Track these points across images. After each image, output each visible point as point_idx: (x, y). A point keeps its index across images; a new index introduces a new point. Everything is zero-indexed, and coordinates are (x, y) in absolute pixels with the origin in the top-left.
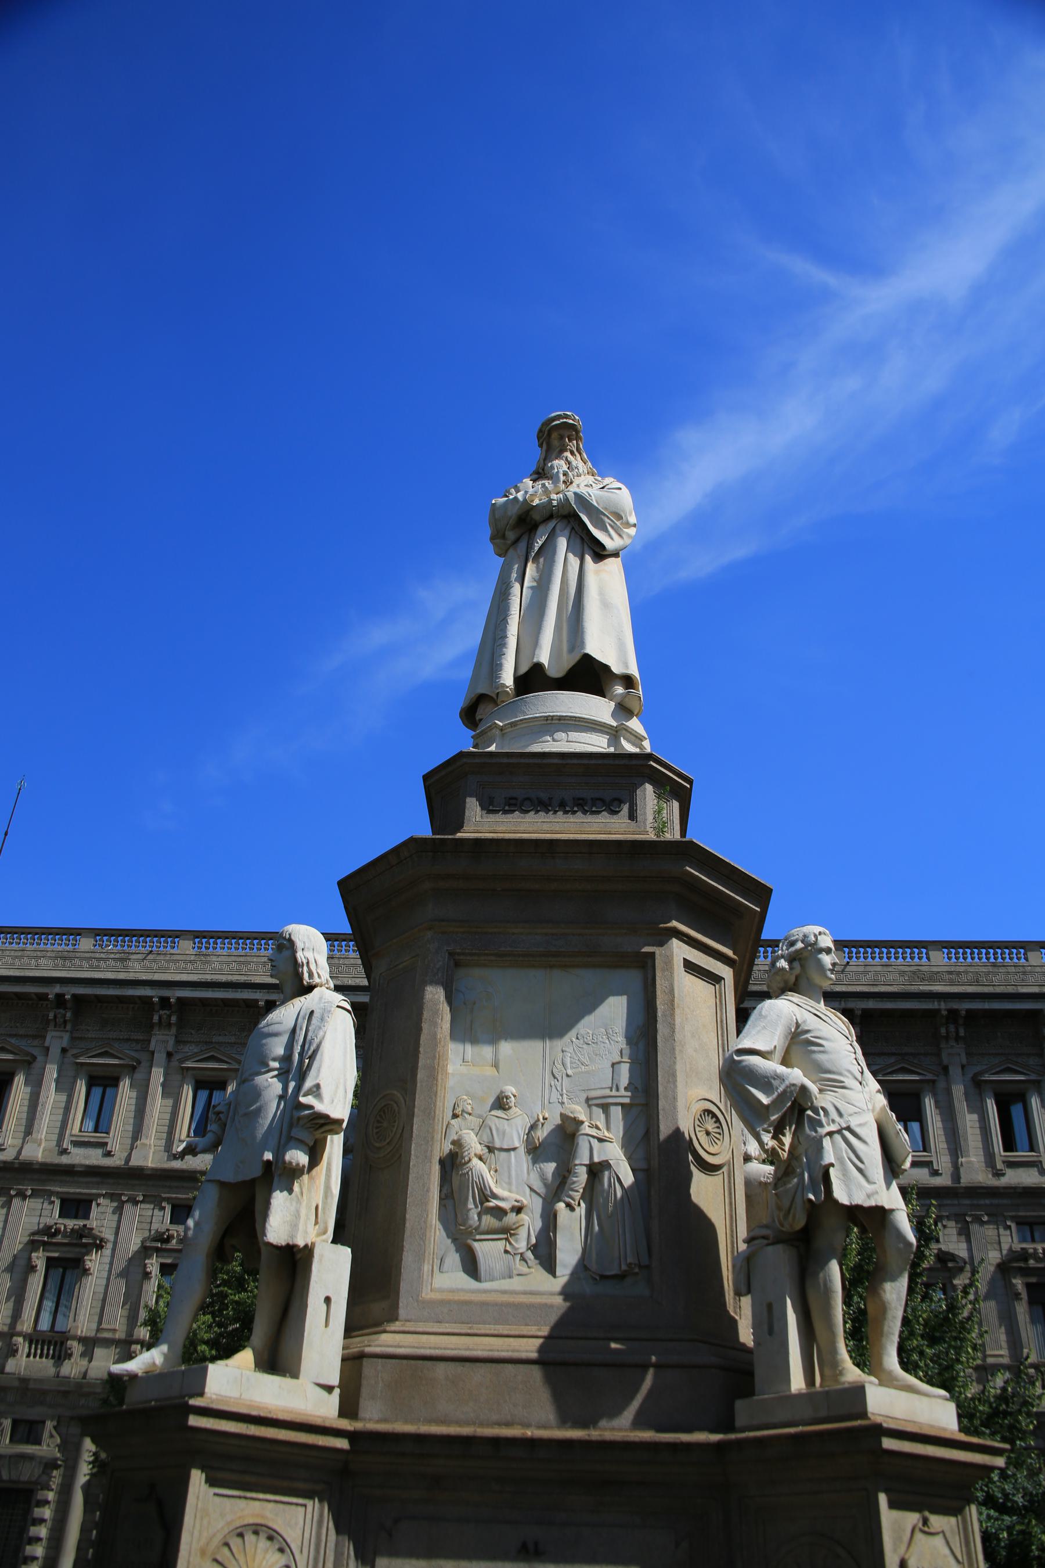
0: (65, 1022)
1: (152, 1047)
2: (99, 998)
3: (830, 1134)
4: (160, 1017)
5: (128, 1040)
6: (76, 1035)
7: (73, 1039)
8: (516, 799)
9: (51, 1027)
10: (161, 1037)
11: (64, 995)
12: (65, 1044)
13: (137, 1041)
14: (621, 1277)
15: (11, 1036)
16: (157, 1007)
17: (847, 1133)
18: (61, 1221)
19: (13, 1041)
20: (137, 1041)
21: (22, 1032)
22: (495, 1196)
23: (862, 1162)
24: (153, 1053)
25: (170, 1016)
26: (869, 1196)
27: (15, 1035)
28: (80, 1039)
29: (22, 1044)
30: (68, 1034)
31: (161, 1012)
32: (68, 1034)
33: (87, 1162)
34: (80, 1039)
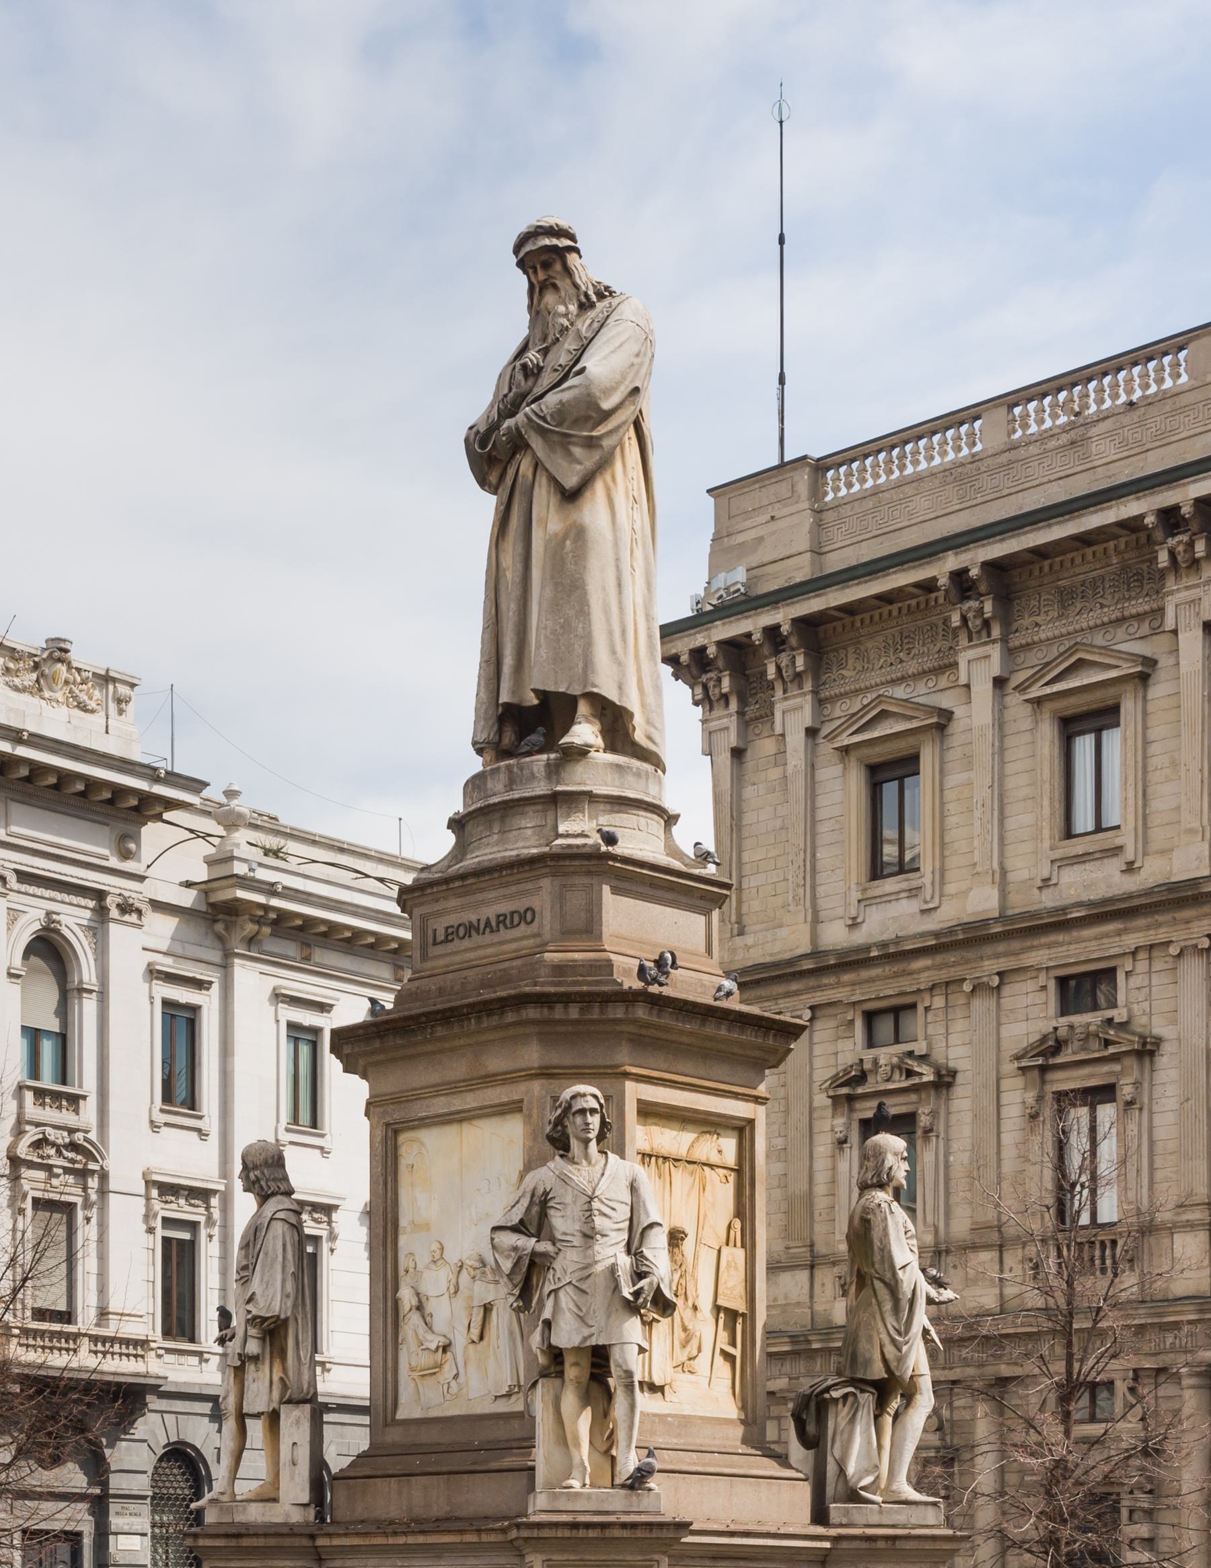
0: (986, 624)
1: (1169, 623)
2: (1040, 553)
3: (556, 1291)
4: (1172, 554)
5: (1122, 620)
6: (1016, 640)
7: (1010, 653)
9: (963, 641)
10: (1183, 595)
11: (966, 570)
12: (996, 671)
13: (1139, 617)
14: (508, 1395)
15: (894, 682)
16: (1159, 535)
17: (569, 1289)
18: (1064, 1021)
19: (900, 692)
20: (1139, 617)
21: (912, 667)
23: (580, 1310)
24: (1175, 632)
25: (1191, 545)
26: (585, 1339)
27: (902, 679)
28: (1027, 647)
29: (921, 693)
30: (998, 646)
31: (1171, 542)
32: (998, 646)
33: (1093, 896)
34: (1027, 647)
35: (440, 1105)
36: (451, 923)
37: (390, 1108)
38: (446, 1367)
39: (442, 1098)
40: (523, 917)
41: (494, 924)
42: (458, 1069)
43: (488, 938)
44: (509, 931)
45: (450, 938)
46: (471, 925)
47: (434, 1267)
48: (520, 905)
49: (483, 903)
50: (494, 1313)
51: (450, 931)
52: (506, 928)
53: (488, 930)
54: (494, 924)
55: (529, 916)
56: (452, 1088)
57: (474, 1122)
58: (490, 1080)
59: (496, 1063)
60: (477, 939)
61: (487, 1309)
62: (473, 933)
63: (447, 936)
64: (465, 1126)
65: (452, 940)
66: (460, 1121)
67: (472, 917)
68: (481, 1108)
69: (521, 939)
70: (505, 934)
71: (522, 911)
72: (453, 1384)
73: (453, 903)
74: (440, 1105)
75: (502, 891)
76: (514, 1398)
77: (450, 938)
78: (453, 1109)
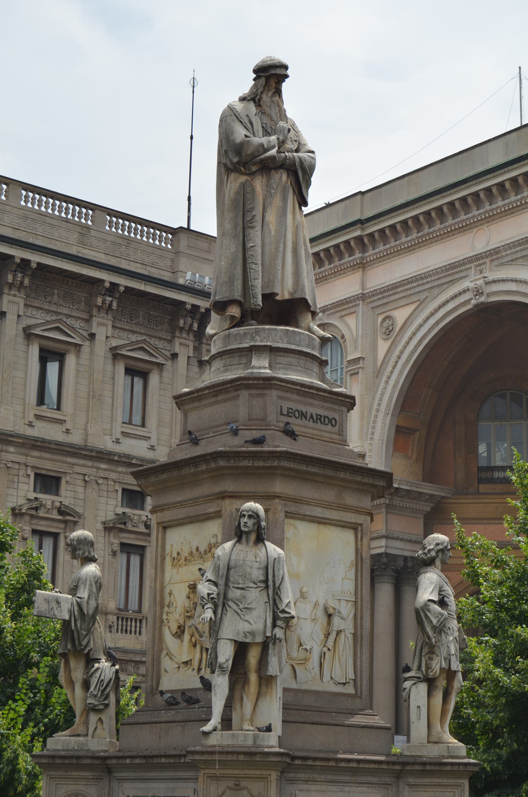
8: (292, 409)
22: (305, 644)
35: (318, 512)
36: (291, 407)
37: (289, 503)
38: (311, 660)
39: (320, 508)
40: (330, 421)
41: (315, 418)
42: (329, 495)
43: (311, 424)
44: (323, 426)
45: (290, 415)
46: (302, 414)
47: (304, 602)
48: (331, 415)
49: (311, 405)
50: (342, 636)
51: (290, 411)
52: (321, 423)
53: (311, 420)
54: (315, 418)
55: (333, 422)
56: (328, 506)
57: (327, 526)
58: (347, 508)
59: (350, 499)
60: (304, 422)
61: (339, 633)
62: (303, 418)
63: (288, 412)
64: (322, 527)
65: (291, 417)
66: (320, 523)
67: (303, 409)
68: (338, 521)
69: (326, 432)
70: (319, 425)
71: (330, 418)
72: (312, 671)
73: (295, 397)
74: (318, 512)
75: (322, 403)
76: (347, 685)
77: (290, 415)
78: (326, 516)
